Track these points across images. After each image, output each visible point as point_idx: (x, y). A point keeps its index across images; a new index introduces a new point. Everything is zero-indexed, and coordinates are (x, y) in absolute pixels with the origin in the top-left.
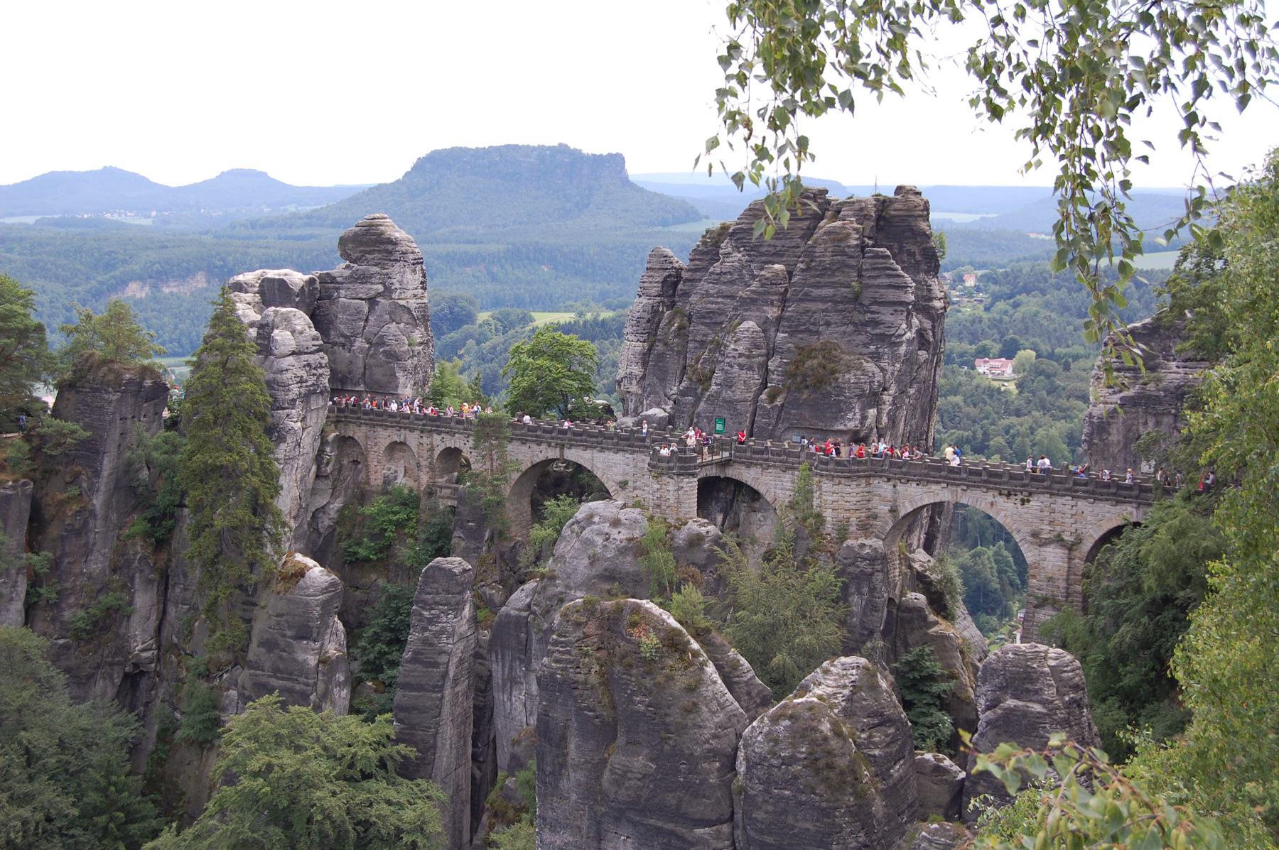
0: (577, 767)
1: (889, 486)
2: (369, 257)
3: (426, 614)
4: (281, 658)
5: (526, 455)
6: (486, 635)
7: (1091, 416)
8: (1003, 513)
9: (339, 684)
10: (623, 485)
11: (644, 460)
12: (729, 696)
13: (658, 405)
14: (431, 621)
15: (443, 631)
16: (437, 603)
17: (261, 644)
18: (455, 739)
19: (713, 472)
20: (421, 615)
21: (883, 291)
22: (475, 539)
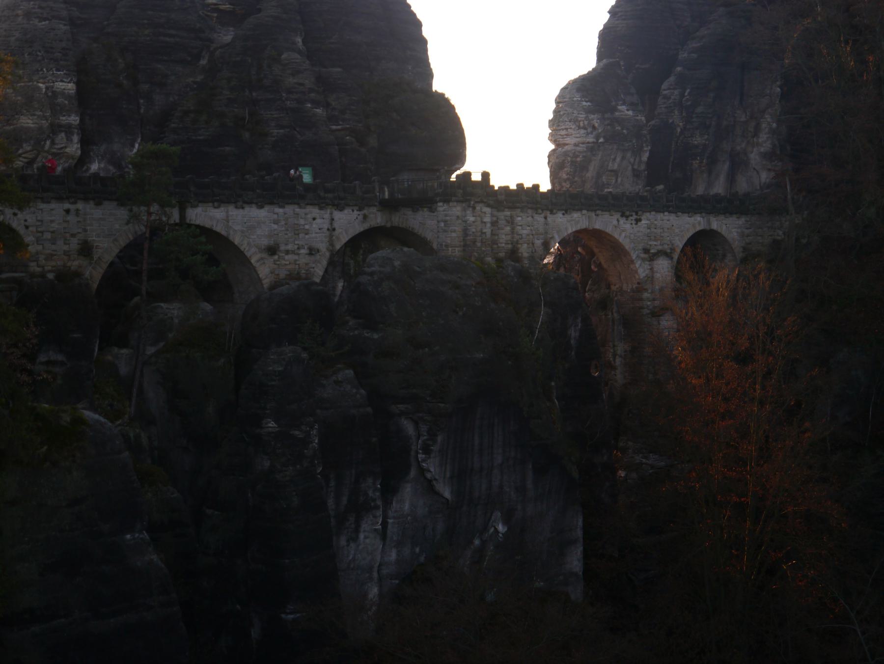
8: (623, 235)
10: (272, 250)
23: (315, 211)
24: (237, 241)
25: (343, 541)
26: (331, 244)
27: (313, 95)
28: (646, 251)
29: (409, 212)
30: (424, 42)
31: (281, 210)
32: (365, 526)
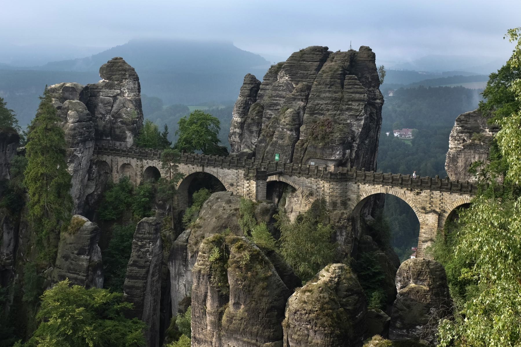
0: (211, 314)
1: (356, 186)
2: (114, 77)
3: (139, 243)
4: (71, 264)
5: (186, 169)
6: (166, 254)
7: (449, 154)
8: (408, 199)
9: (98, 276)
10: (232, 185)
11: (242, 172)
12: (281, 281)
13: (249, 147)
14: (142, 246)
15: (148, 251)
16: (145, 239)
18: (152, 302)
19: (274, 178)
20: (137, 244)
21: (353, 95)
22: (162, 209)
28: (424, 208)
31: (236, 171)
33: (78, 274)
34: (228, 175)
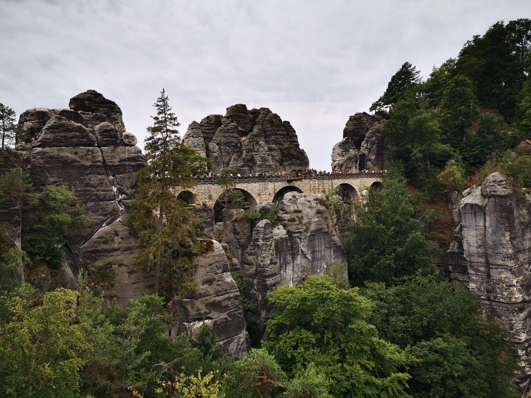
2: (101, 109)
4: (219, 285)
17: (205, 282)
20: (266, 244)
23: (270, 183)
24: (249, 192)
25: (282, 272)
26: (275, 192)
27: (268, 152)
29: (295, 182)
30: (297, 136)
32: (287, 268)
33: (228, 293)
34: (255, 187)
